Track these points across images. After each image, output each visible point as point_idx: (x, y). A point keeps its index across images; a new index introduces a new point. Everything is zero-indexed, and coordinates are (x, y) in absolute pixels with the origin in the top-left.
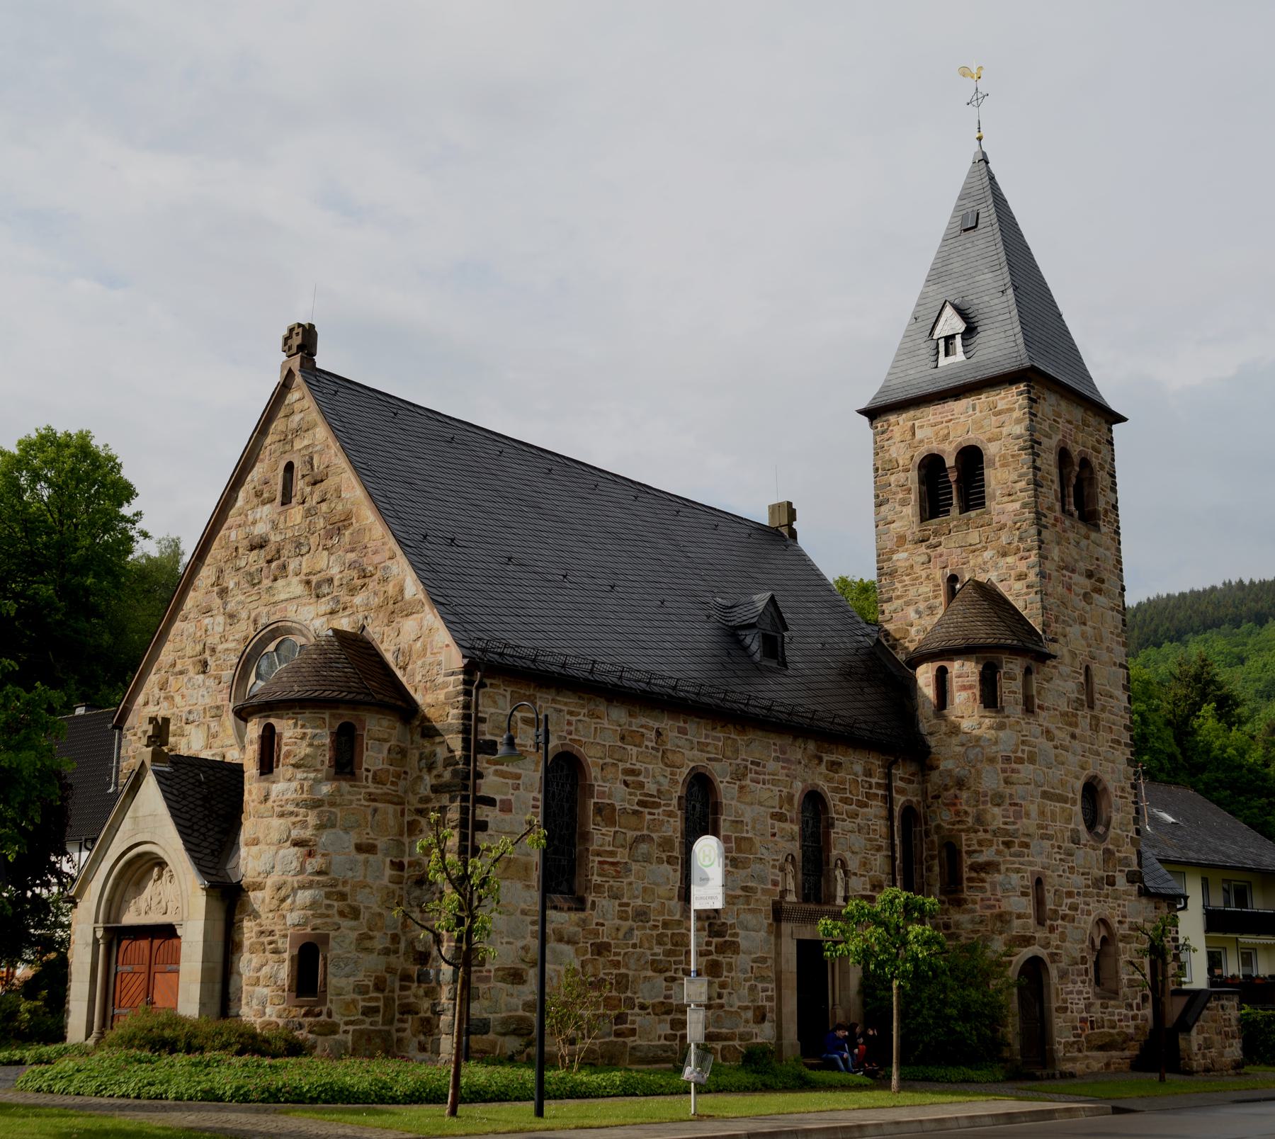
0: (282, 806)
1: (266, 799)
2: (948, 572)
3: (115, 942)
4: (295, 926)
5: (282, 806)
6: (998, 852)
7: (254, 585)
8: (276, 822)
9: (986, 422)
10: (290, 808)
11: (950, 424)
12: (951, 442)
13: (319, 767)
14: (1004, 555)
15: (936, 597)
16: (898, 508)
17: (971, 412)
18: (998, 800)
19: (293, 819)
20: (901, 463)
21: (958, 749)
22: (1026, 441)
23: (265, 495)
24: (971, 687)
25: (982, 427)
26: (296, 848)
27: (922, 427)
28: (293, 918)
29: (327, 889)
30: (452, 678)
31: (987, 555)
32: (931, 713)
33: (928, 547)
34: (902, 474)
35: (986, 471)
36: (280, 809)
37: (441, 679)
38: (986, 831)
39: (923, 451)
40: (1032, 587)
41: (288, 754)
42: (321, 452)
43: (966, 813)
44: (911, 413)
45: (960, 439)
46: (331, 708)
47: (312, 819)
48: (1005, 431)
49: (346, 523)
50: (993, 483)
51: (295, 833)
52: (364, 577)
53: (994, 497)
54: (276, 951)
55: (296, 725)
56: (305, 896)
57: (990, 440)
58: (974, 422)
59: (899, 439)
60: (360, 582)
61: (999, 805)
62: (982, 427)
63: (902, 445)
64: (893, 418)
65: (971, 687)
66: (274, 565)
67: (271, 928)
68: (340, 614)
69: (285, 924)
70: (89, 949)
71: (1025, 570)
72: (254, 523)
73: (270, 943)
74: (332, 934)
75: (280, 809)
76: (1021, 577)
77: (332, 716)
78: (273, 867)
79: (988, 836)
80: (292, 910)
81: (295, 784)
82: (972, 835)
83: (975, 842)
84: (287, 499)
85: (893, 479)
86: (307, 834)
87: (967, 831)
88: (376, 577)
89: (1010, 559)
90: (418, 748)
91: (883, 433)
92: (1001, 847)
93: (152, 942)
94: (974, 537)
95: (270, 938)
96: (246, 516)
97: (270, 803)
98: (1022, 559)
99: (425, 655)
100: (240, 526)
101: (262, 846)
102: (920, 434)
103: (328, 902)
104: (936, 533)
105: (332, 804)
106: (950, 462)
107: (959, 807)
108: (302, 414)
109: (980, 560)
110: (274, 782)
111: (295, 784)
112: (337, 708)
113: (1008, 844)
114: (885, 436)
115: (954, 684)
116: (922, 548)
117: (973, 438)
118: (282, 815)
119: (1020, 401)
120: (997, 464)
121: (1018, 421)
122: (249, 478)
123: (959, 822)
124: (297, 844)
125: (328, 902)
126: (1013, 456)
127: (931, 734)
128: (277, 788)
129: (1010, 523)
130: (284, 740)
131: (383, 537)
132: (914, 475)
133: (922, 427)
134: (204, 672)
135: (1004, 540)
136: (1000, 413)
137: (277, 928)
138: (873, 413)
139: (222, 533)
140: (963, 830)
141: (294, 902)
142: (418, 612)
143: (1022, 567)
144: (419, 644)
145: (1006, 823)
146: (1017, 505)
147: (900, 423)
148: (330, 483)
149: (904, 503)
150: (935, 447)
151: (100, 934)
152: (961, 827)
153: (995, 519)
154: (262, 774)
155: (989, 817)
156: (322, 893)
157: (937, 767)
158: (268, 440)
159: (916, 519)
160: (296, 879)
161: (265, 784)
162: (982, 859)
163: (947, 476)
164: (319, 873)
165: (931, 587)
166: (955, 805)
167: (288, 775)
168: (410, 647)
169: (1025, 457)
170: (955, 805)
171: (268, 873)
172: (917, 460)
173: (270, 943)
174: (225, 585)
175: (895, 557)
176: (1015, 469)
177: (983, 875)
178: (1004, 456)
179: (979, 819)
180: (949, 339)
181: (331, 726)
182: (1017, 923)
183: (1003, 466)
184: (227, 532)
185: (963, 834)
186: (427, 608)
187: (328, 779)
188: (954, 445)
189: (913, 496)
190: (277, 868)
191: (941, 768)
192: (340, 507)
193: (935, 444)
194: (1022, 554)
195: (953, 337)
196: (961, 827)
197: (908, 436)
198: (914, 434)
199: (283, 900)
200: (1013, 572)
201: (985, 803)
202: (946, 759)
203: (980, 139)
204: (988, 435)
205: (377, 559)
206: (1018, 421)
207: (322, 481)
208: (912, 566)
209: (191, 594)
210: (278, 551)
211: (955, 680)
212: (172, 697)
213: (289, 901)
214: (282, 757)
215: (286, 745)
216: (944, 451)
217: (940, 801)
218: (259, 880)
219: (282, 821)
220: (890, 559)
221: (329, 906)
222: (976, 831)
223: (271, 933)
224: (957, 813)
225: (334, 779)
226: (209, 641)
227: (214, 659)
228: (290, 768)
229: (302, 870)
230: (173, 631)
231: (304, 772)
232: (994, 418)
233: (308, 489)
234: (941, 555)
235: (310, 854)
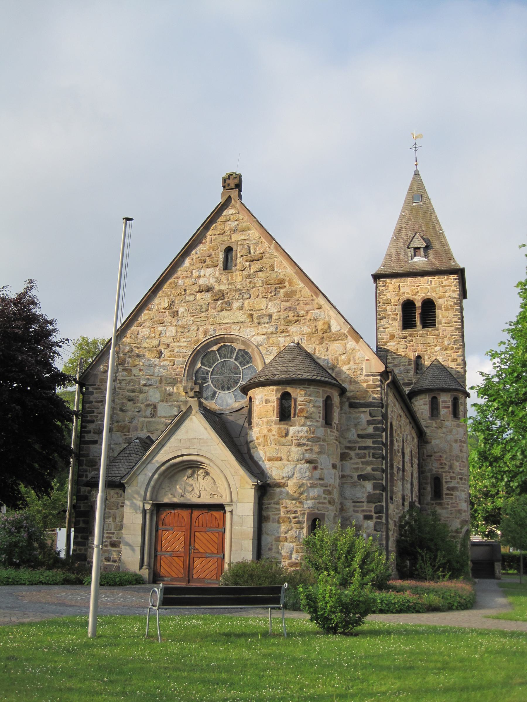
0: (298, 440)
1: (287, 435)
2: (416, 354)
3: (155, 512)
4: (309, 508)
5: (298, 440)
6: (458, 483)
7: (202, 312)
8: (294, 449)
9: (437, 289)
10: (303, 441)
11: (419, 287)
12: (419, 296)
13: (318, 419)
14: (446, 349)
15: (409, 365)
16: (390, 322)
17: (429, 284)
18: (457, 458)
19: (305, 448)
20: (393, 301)
21: (442, 435)
22: (457, 301)
23: (207, 263)
24: (448, 407)
25: (435, 291)
26: (308, 465)
27: (404, 286)
28: (309, 503)
29: (324, 488)
30: (371, 378)
31: (437, 349)
32: (427, 418)
33: (406, 342)
34: (394, 307)
35: (437, 311)
36: (297, 441)
37: (362, 377)
38: (453, 473)
39: (404, 298)
40: (460, 365)
41: (302, 411)
42: (256, 245)
43: (445, 464)
44: (398, 280)
45: (424, 295)
46: (323, 387)
47: (316, 449)
48: (447, 295)
49: (281, 285)
50: (440, 317)
51: (308, 456)
52: (298, 316)
53: (440, 323)
54: (298, 522)
55: (305, 394)
56: (314, 492)
57: (439, 298)
58: (432, 288)
59: (392, 291)
60: (295, 319)
61: (458, 461)
62: (435, 291)
63: (394, 293)
64: (388, 280)
65: (448, 407)
66: (219, 302)
67: (294, 509)
68: (278, 335)
69: (303, 507)
70: (140, 516)
71: (456, 357)
72: (199, 277)
73: (295, 518)
74: (326, 513)
75: (297, 441)
76: (454, 360)
77: (323, 391)
78: (293, 474)
79: (454, 475)
80: (307, 500)
81: (305, 428)
82: (448, 474)
83: (449, 477)
84: (226, 267)
85: (388, 308)
86: (313, 456)
87: (446, 472)
88: (308, 318)
89: (448, 352)
90: (345, 413)
91: (383, 286)
92: (459, 480)
93: (192, 513)
94: (430, 339)
95: (294, 515)
96: (192, 272)
97: (289, 437)
98: (454, 352)
99: (349, 363)
100: (187, 277)
101: (285, 462)
102: (402, 290)
103: (324, 496)
104: (410, 335)
105: (324, 440)
106: (418, 304)
107: (442, 461)
108: (236, 223)
109: (433, 350)
110: (291, 426)
111: (305, 428)
112: (325, 387)
113: (461, 479)
114: (384, 288)
115: (441, 405)
116: (403, 342)
117: (430, 295)
118: (298, 445)
119: (455, 283)
120: (443, 309)
121: (454, 291)
122: (194, 252)
123: (442, 468)
124: (309, 462)
125: (324, 496)
126: (451, 306)
127: (426, 427)
128: (292, 430)
129: (449, 336)
130: (298, 403)
131: (312, 296)
132: (399, 308)
133: (404, 286)
134: (159, 358)
135: (446, 343)
136: (445, 286)
137: (298, 509)
138: (376, 277)
139: (172, 280)
140: (444, 472)
141: (308, 494)
142: (342, 340)
143: (455, 356)
144: (343, 357)
145: (460, 470)
146: (453, 328)
147: (392, 283)
148: (265, 261)
149: (394, 320)
150: (411, 297)
151: (148, 507)
152: (442, 470)
153: (441, 333)
154: (280, 420)
155: (455, 467)
156: (322, 491)
157: (431, 442)
158: (210, 233)
159: (400, 328)
160: (308, 482)
161: (283, 427)
162: (452, 485)
163: (415, 310)
164: (321, 479)
165: (407, 360)
166: (440, 460)
167: (302, 423)
168: (337, 358)
169: (456, 307)
170: (440, 460)
171: (289, 478)
172: (401, 301)
173: (295, 518)
174: (175, 309)
175: (388, 344)
176: (452, 313)
177: (452, 492)
178: (447, 306)
179: (451, 467)
180: (416, 249)
181: (323, 397)
182: (464, 514)
183: (446, 310)
184: (176, 280)
185: (444, 474)
186: (349, 338)
187: (322, 427)
188: (421, 297)
189: (398, 317)
190: (297, 475)
191: (433, 443)
192: (274, 276)
193: (410, 295)
194: (454, 350)
195: (419, 248)
196: (442, 470)
197: (397, 289)
198: (400, 289)
199: (301, 494)
200: (450, 358)
201: (453, 460)
202: (436, 439)
203: (416, 165)
204: (439, 295)
205: (307, 308)
206: (454, 291)
207: (259, 260)
208: (397, 350)
209: (146, 312)
210: (223, 295)
211: (441, 403)
212: (131, 370)
213: (305, 494)
214: (297, 411)
215: (300, 405)
216: (416, 299)
217: (432, 458)
218: (283, 481)
219: (298, 448)
220: (385, 345)
221: (325, 498)
222: (450, 472)
223: (295, 512)
224: (441, 464)
225: (325, 427)
226: (163, 340)
227: (168, 350)
228: (303, 420)
229: (310, 478)
230: (129, 332)
231: (311, 421)
232: (441, 288)
233: (247, 264)
234: (413, 346)
235: (315, 468)
